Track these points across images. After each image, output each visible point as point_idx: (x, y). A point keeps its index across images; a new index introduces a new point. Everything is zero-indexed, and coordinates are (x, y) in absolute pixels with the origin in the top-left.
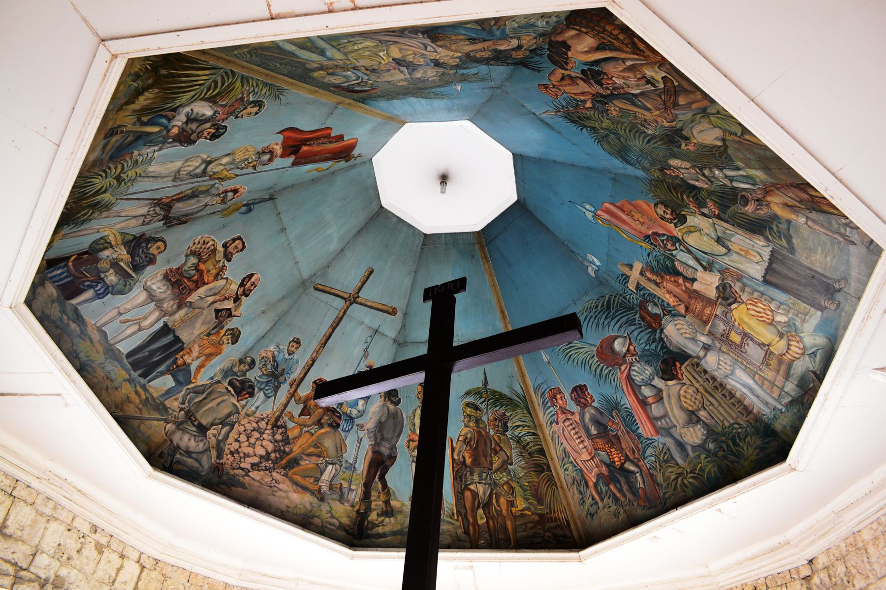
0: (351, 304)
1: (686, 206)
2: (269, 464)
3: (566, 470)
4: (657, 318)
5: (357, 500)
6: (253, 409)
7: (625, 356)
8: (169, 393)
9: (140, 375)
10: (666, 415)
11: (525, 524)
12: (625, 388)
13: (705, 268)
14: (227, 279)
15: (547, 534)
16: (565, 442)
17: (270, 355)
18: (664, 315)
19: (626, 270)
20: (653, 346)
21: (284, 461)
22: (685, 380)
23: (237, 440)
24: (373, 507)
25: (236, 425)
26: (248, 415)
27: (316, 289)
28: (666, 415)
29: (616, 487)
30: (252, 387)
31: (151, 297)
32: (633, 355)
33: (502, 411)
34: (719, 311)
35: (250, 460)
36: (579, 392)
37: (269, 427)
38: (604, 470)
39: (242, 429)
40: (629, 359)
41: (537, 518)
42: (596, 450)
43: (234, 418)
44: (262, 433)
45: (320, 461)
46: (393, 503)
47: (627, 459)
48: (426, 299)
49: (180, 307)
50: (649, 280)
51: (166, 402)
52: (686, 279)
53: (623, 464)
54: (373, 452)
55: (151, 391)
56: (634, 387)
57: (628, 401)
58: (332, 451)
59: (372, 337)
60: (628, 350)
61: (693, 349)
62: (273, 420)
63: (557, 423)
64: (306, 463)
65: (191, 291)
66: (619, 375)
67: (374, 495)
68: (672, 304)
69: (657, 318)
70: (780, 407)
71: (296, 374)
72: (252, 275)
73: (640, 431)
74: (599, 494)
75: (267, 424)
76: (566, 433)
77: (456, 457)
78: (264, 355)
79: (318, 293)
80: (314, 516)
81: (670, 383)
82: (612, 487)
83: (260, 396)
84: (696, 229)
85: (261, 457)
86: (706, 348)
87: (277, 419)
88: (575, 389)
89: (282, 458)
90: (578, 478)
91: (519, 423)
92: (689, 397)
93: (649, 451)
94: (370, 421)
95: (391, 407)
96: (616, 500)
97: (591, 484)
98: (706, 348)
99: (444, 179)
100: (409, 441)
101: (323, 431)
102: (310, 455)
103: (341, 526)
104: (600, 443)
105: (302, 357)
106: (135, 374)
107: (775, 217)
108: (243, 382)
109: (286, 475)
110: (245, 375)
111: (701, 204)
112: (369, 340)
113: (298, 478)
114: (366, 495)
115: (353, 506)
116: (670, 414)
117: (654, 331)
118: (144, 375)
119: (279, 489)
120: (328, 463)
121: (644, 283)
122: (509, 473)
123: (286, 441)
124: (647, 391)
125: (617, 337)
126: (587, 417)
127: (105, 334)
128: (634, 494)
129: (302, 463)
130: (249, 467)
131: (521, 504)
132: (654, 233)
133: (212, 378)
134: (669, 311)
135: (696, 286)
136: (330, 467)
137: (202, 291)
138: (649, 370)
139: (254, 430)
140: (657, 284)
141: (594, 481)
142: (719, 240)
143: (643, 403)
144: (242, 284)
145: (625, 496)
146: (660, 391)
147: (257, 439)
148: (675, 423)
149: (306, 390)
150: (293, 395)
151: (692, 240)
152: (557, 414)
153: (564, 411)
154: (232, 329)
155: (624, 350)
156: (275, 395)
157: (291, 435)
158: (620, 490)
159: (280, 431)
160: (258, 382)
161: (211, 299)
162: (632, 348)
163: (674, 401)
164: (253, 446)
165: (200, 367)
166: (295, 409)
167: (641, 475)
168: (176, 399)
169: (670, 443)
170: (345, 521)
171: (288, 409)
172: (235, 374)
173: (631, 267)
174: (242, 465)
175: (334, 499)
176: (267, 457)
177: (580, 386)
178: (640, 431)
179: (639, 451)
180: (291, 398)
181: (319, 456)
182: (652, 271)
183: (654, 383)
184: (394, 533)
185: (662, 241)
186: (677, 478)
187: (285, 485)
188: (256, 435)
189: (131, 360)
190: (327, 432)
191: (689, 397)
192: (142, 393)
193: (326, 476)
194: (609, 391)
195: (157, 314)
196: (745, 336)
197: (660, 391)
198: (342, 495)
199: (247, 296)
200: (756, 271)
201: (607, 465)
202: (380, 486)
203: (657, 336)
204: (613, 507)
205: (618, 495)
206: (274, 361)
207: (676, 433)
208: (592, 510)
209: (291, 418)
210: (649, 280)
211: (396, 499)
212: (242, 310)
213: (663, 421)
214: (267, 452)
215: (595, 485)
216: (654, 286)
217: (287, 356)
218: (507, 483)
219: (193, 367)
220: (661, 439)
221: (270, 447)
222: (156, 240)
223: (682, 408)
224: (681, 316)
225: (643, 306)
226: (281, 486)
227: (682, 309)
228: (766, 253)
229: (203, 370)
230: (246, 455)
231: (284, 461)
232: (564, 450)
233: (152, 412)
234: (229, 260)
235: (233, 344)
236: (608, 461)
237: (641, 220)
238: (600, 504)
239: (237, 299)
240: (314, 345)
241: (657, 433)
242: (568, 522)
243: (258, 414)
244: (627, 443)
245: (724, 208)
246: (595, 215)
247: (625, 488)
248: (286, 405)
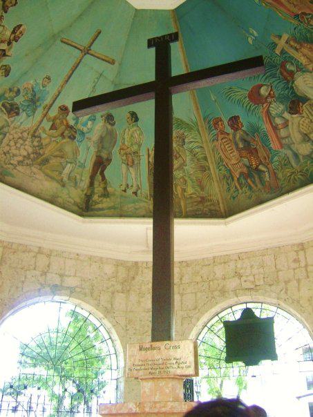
0: (85, 54)
2: (29, 162)
4: (292, 74)
5: (86, 187)
6: (19, 123)
7: (266, 98)
10: (288, 136)
11: (192, 203)
12: (264, 119)
14: (4, 26)
15: (205, 209)
16: (221, 154)
17: (30, 87)
18: (297, 71)
19: (276, 40)
20: (286, 92)
21: (39, 160)
22: (304, 114)
23: (8, 145)
24: (96, 191)
25: (8, 135)
26: (15, 128)
27: (62, 41)
28: (288, 136)
29: (252, 181)
30: (18, 108)
32: (272, 97)
33: (182, 131)
35: (16, 158)
36: (234, 121)
37: (30, 136)
38: (245, 170)
39: (11, 137)
40: (269, 100)
41: (200, 199)
43: (6, 130)
44: (25, 141)
45: (62, 160)
46: (109, 189)
47: (261, 163)
48: (150, 46)
54: (97, 156)
57: (265, 127)
58: (70, 155)
59: (98, 79)
60: (269, 94)
62: (32, 132)
63: (217, 140)
64: (53, 161)
66: (261, 110)
67: (96, 184)
69: (292, 74)
71: (48, 101)
72: (21, 25)
74: (240, 184)
75: (28, 134)
77: (151, 160)
78: (26, 86)
79: (63, 45)
80: (58, 197)
81: (294, 116)
82: (249, 181)
83: (23, 115)
85: (24, 157)
87: (35, 132)
88: (231, 119)
89: (37, 158)
90: (228, 174)
91: (192, 140)
92: (305, 125)
93: (276, 158)
94: (95, 137)
95: (109, 127)
96: (251, 188)
100: (121, 149)
101: (65, 141)
102: (56, 156)
103: (76, 204)
104: (244, 153)
105: (52, 89)
108: (12, 105)
109: (40, 169)
110: (13, 100)
112: (96, 80)
113: (48, 172)
114: (92, 184)
115: (83, 191)
116: (292, 135)
117: (288, 82)
119: (36, 178)
120: (67, 162)
121: (287, 49)
122: (184, 171)
123: (41, 146)
124: (279, 121)
125: (262, 86)
126: (238, 137)
129: (51, 162)
130: (16, 163)
131: (190, 190)
132: (303, 13)
136: (69, 165)
138: (282, 107)
139: (20, 138)
140: (297, 49)
143: (275, 128)
144: (14, 32)
145: (257, 186)
146: (288, 121)
147: (22, 145)
148: (294, 141)
149: (54, 112)
150: (45, 115)
153: (222, 132)
154: (6, 66)
155: (267, 94)
156: (34, 115)
157: (45, 142)
158: (254, 182)
159: (37, 139)
160: (22, 105)
162: (272, 92)
163: (295, 126)
164: (19, 149)
166: (47, 125)
167: (269, 173)
169: (289, 153)
170: (78, 200)
171: (42, 125)
172: (6, 99)
173: (280, 37)
174: (12, 162)
175: (70, 186)
176: (28, 157)
177: (234, 117)
179: (269, 158)
180: (43, 118)
181: (62, 157)
182: (295, 40)
183: (284, 116)
184: (110, 208)
185: (308, 19)
186: (291, 175)
187: (41, 176)
188: (21, 141)
190: (67, 142)
191: (305, 125)
193: (67, 171)
194: (253, 120)
197: (287, 121)
198: (76, 183)
199: (16, 41)
201: (248, 167)
202: (100, 178)
203: (290, 84)
205: (252, 185)
206: (33, 91)
207: (294, 148)
208: (234, 195)
209: (44, 130)
211: (111, 187)
213: (287, 140)
214: (28, 153)
215: (238, 179)
216: (295, 52)
217: (41, 88)
218: (182, 177)
220: (285, 151)
221: (30, 150)
223: (300, 132)
224: (308, 72)
225: (283, 65)
226: (37, 176)
230: (14, 155)
231: (39, 160)
232: (220, 158)
234: (6, 12)
235: (6, 76)
236: (248, 164)
237: (295, 3)
238: (240, 191)
239: (9, 43)
240: (60, 82)
241: (282, 147)
242: (218, 201)
243: (22, 127)
244: (262, 153)
248: (41, 122)
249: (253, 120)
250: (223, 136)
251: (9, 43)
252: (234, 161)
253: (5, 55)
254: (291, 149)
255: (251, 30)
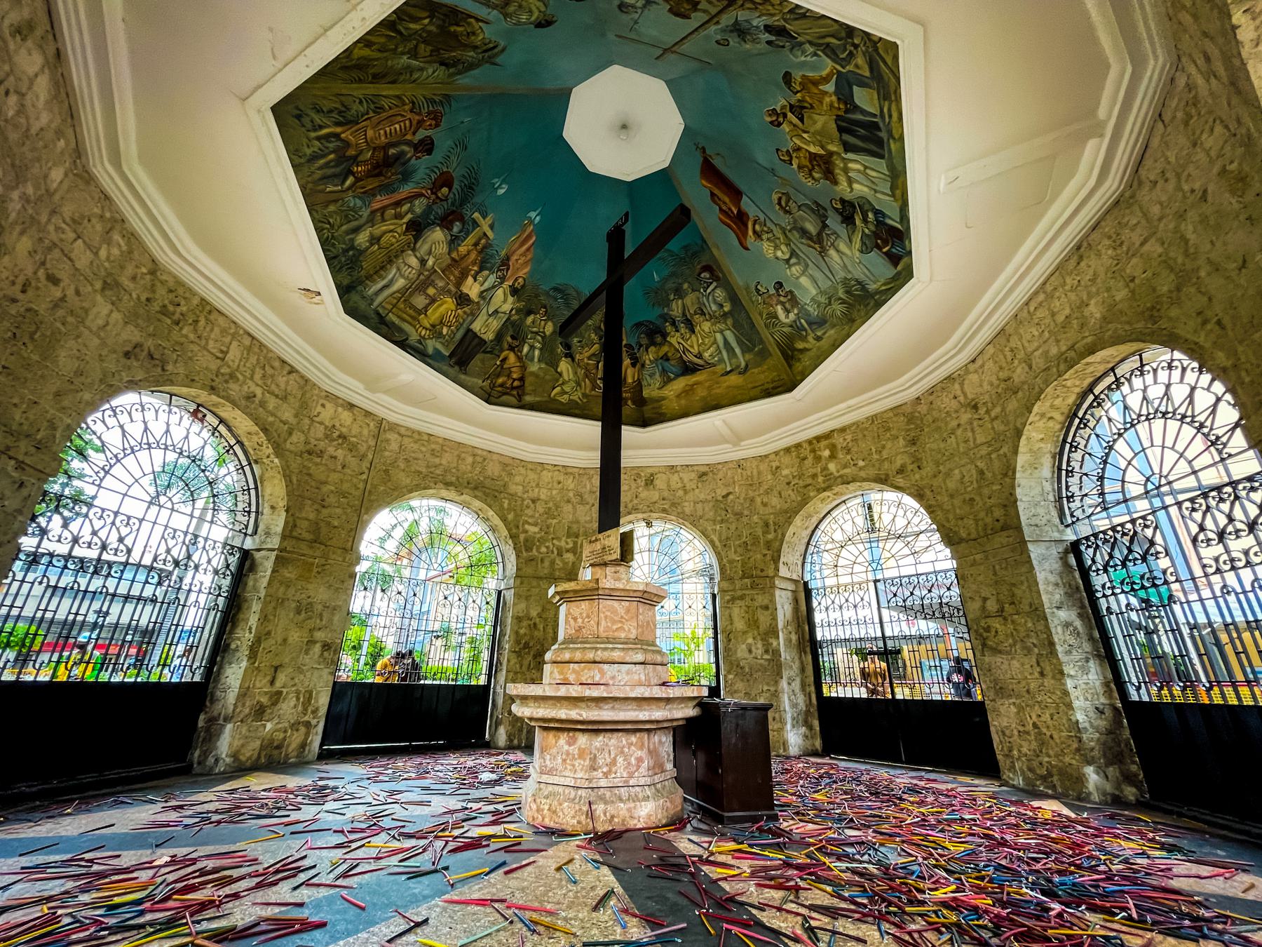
1: (519, 301)
3: (361, 102)
8: (862, 84)
9: (879, 129)
13: (482, 292)
16: (391, 112)
19: (489, 220)
28: (383, 220)
29: (331, 161)
31: (850, 181)
34: (453, 289)
36: (426, 146)
38: (351, 152)
40: (433, 197)
42: (375, 149)
47: (358, 180)
49: (831, 154)
50: (480, 239)
51: (867, 74)
52: (477, 273)
53: (353, 174)
55: (876, 102)
56: (411, 198)
57: (406, 190)
61: (423, 248)
63: (411, 111)
65: (821, 156)
68: (460, 249)
70: (376, 304)
72: (772, 123)
73: (379, 197)
76: (400, 119)
82: (332, 156)
84: (505, 301)
86: (423, 262)
88: (432, 143)
90: (349, 115)
93: (359, 203)
97: (338, 130)
98: (423, 262)
99: (624, 127)
106: (883, 135)
107: (502, 351)
111: (519, 311)
118: (875, 126)
124: (406, 207)
127: (892, 189)
128: (321, 179)
133: (815, 54)
134: (454, 242)
135: (470, 279)
137: (813, 149)
138: (418, 210)
140: (476, 244)
141: (343, 136)
142: (496, 312)
143: (398, 204)
151: (500, 292)
152: (419, 114)
153: (420, 123)
158: (327, 165)
161: (805, 135)
165: (826, 80)
168: (857, 66)
173: (492, 227)
178: (379, 197)
182: (485, 247)
189: (880, 151)
192: (885, 110)
195: (850, 165)
196: (433, 301)
200: (477, 326)
201: (355, 157)
204: (308, 151)
205: (322, 161)
208: (306, 120)
210: (480, 239)
212: (783, 102)
215: (337, 136)
216: (473, 241)
219: (830, 87)
220: (365, 213)
222: (836, 209)
223: (385, 233)
225: (461, 219)
227: (454, 255)
228: (484, 337)
229: (824, 73)
233: (886, 78)
236: (360, 159)
238: (313, 135)
241: (373, 212)
244: (372, 184)
245: (513, 324)
246: (531, 221)
247: (329, 171)
249: (420, 174)
250: (414, 123)
251: (785, 116)
252: (370, 133)
253: (791, 106)
254: (367, 222)
255: (505, 186)
